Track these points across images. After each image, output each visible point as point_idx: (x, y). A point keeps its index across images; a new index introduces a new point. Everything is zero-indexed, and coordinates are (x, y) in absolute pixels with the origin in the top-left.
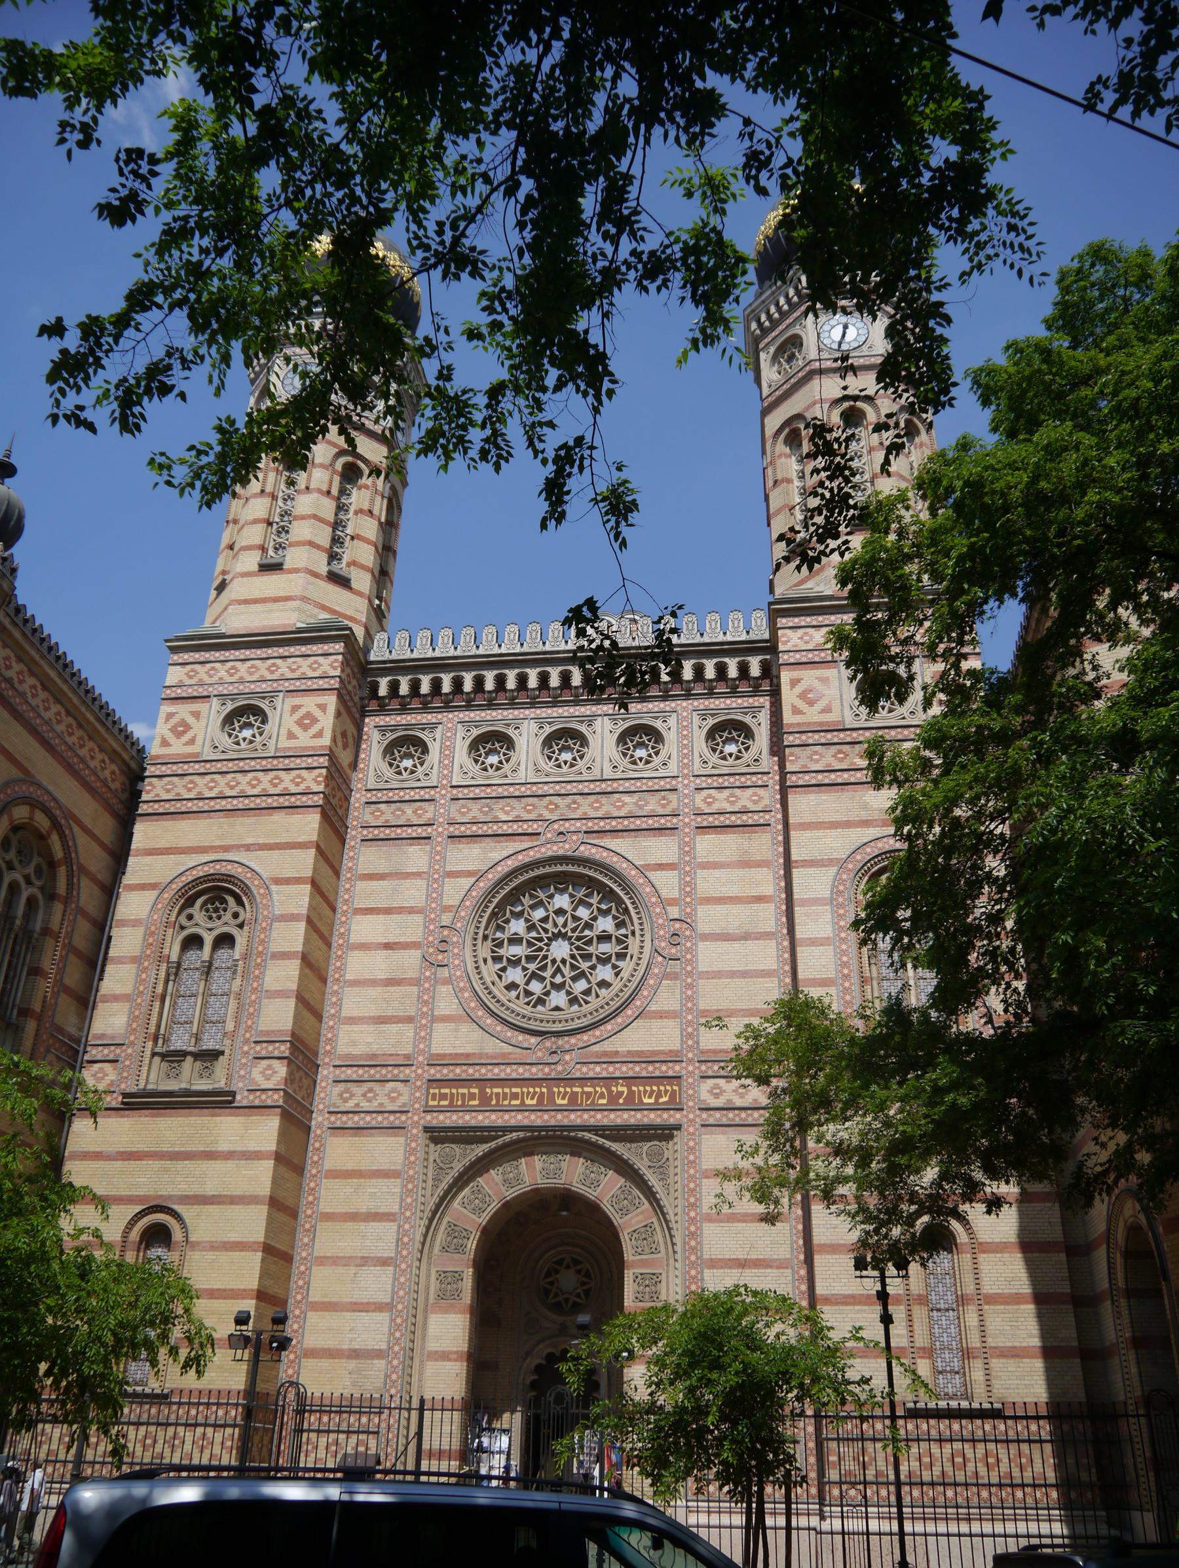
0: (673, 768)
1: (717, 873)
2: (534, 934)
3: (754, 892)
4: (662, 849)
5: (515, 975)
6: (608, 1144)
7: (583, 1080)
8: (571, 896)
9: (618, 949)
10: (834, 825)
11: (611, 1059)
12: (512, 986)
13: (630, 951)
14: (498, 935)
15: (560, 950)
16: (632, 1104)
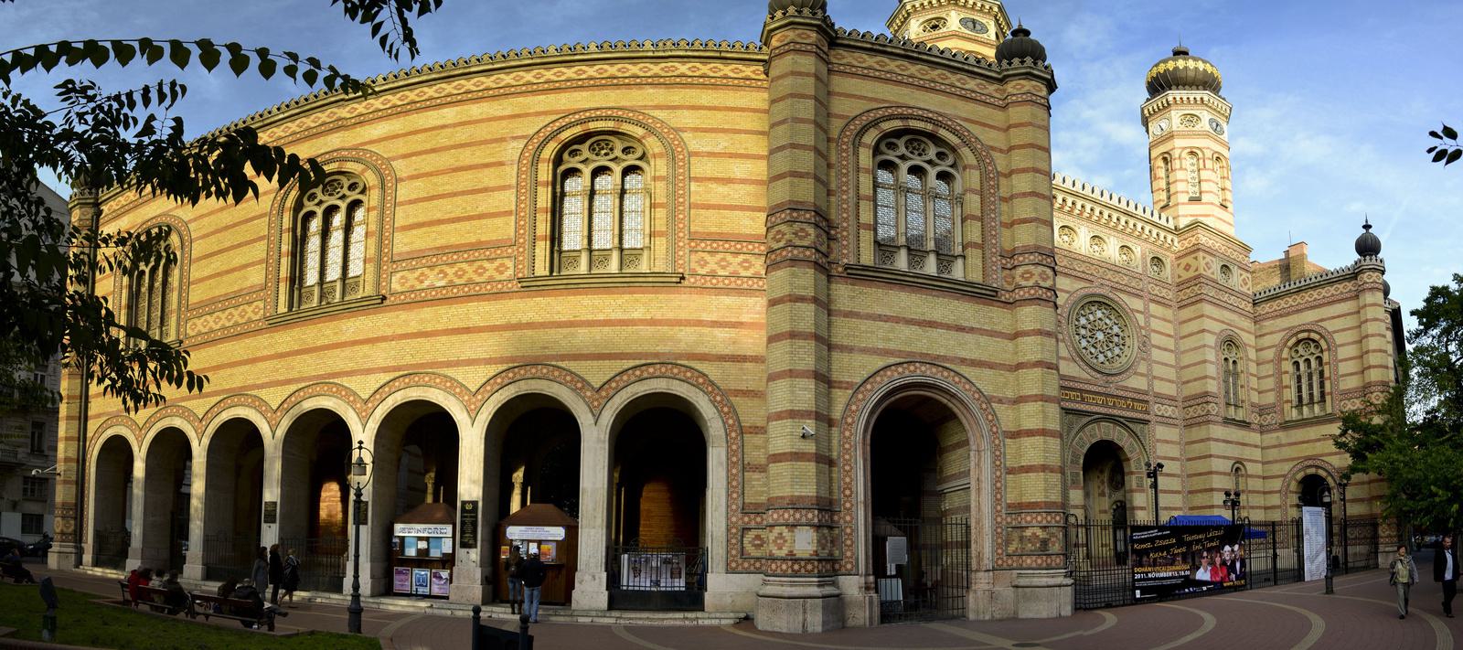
0: (1140, 270)
1: (1157, 320)
2: (1089, 326)
3: (1168, 332)
4: (1136, 304)
5: (1084, 343)
6: (1127, 423)
7: (1117, 396)
8: (1103, 313)
9: (1122, 342)
10: (1215, 319)
11: (1126, 389)
12: (1084, 348)
13: (1127, 344)
14: (1077, 323)
15: (1100, 336)
16: (1133, 409)
